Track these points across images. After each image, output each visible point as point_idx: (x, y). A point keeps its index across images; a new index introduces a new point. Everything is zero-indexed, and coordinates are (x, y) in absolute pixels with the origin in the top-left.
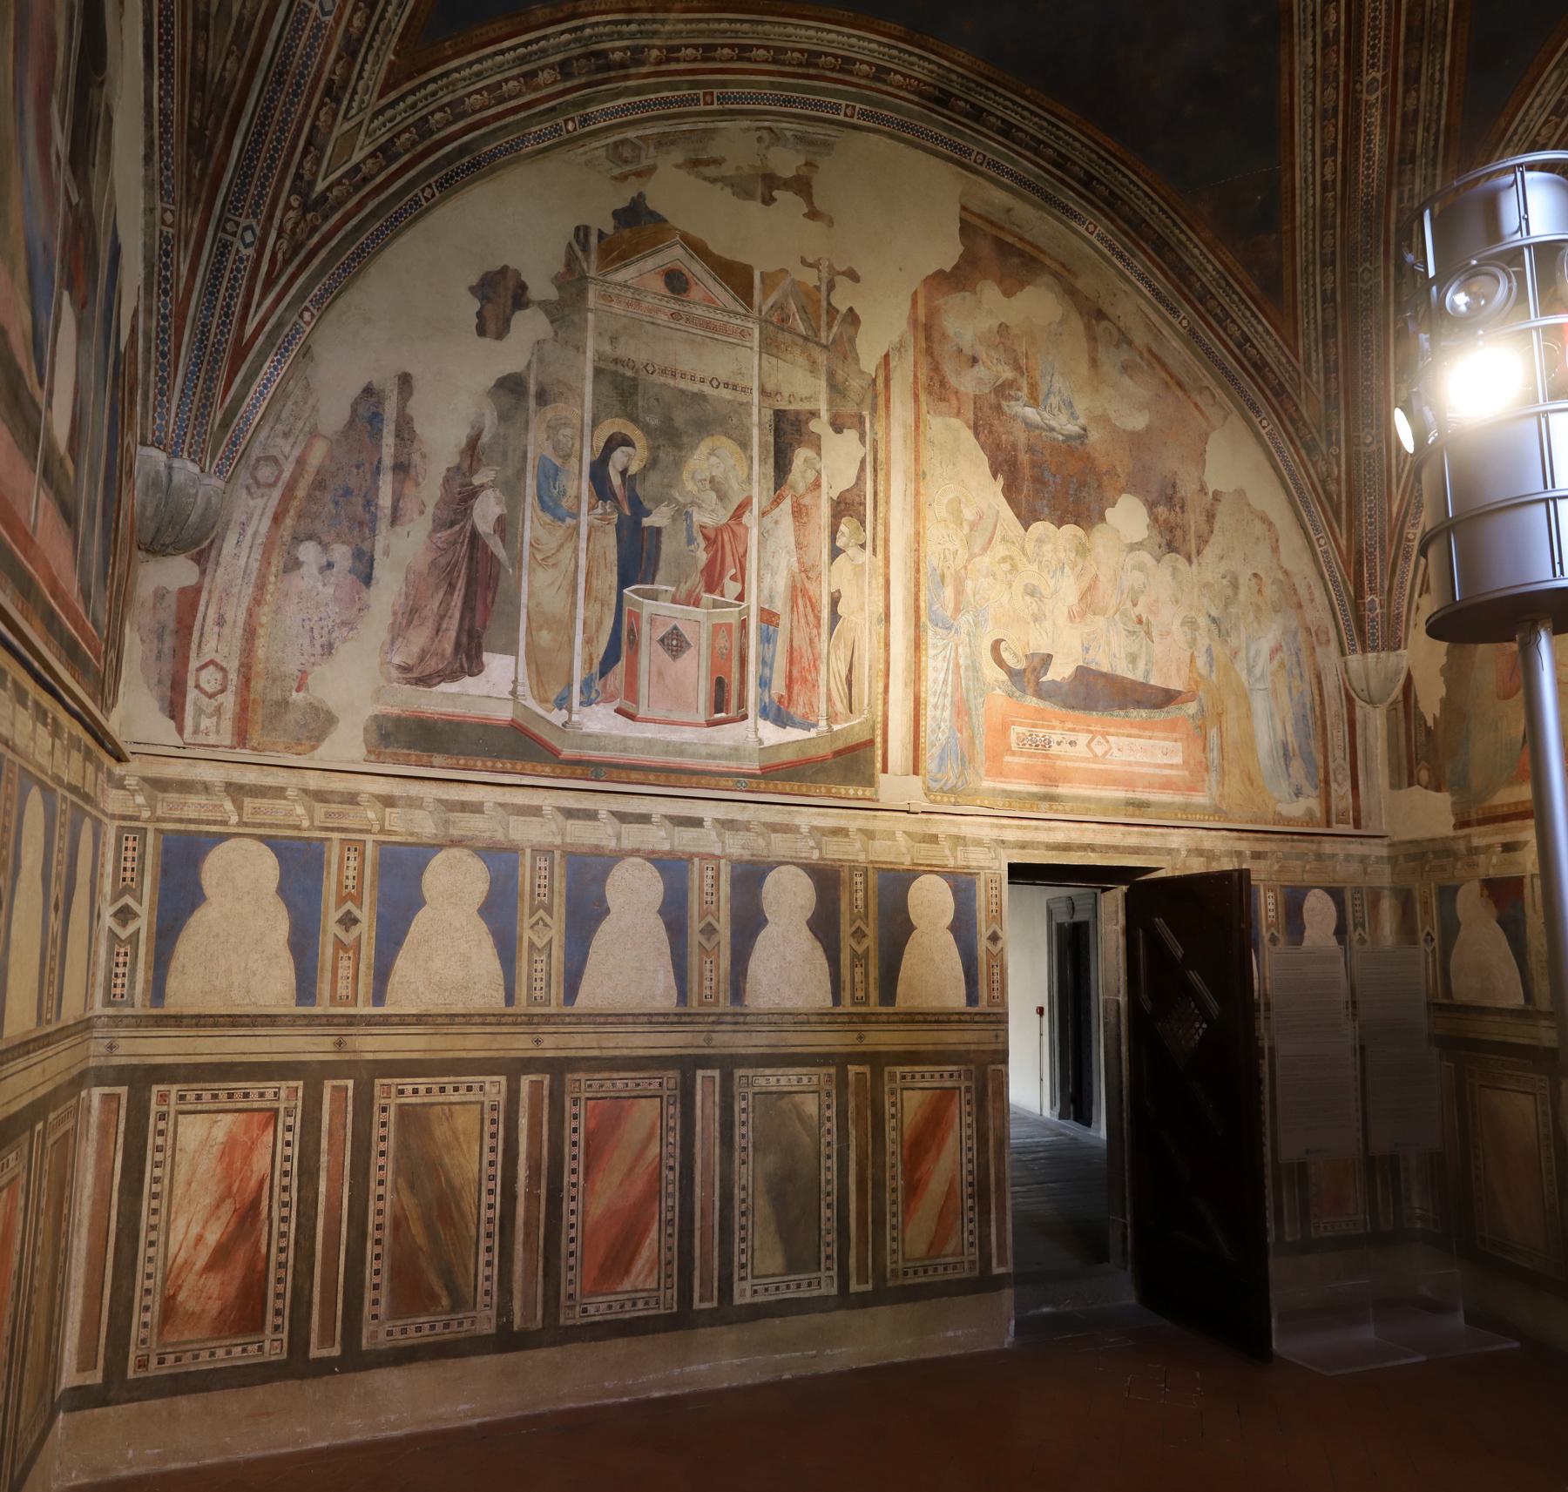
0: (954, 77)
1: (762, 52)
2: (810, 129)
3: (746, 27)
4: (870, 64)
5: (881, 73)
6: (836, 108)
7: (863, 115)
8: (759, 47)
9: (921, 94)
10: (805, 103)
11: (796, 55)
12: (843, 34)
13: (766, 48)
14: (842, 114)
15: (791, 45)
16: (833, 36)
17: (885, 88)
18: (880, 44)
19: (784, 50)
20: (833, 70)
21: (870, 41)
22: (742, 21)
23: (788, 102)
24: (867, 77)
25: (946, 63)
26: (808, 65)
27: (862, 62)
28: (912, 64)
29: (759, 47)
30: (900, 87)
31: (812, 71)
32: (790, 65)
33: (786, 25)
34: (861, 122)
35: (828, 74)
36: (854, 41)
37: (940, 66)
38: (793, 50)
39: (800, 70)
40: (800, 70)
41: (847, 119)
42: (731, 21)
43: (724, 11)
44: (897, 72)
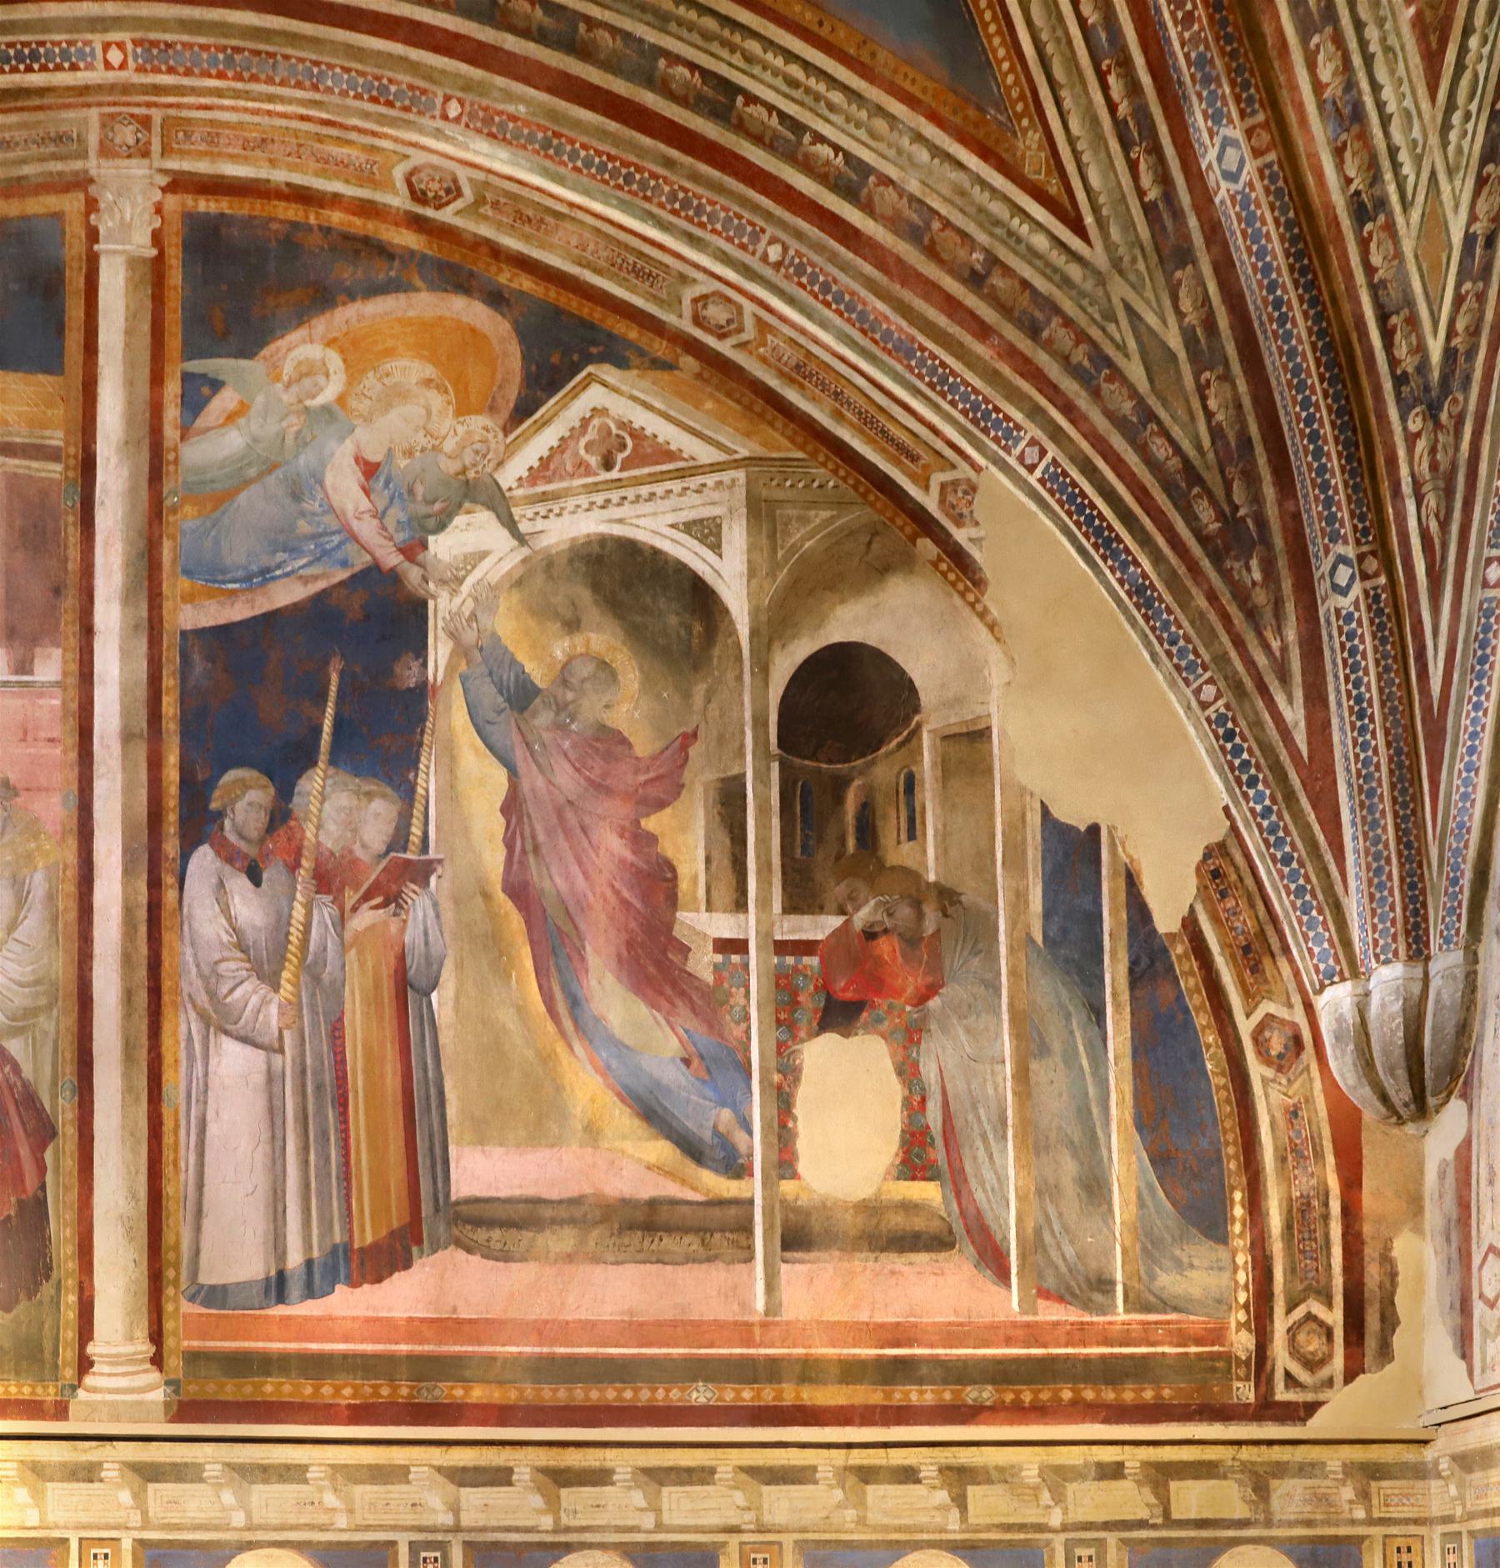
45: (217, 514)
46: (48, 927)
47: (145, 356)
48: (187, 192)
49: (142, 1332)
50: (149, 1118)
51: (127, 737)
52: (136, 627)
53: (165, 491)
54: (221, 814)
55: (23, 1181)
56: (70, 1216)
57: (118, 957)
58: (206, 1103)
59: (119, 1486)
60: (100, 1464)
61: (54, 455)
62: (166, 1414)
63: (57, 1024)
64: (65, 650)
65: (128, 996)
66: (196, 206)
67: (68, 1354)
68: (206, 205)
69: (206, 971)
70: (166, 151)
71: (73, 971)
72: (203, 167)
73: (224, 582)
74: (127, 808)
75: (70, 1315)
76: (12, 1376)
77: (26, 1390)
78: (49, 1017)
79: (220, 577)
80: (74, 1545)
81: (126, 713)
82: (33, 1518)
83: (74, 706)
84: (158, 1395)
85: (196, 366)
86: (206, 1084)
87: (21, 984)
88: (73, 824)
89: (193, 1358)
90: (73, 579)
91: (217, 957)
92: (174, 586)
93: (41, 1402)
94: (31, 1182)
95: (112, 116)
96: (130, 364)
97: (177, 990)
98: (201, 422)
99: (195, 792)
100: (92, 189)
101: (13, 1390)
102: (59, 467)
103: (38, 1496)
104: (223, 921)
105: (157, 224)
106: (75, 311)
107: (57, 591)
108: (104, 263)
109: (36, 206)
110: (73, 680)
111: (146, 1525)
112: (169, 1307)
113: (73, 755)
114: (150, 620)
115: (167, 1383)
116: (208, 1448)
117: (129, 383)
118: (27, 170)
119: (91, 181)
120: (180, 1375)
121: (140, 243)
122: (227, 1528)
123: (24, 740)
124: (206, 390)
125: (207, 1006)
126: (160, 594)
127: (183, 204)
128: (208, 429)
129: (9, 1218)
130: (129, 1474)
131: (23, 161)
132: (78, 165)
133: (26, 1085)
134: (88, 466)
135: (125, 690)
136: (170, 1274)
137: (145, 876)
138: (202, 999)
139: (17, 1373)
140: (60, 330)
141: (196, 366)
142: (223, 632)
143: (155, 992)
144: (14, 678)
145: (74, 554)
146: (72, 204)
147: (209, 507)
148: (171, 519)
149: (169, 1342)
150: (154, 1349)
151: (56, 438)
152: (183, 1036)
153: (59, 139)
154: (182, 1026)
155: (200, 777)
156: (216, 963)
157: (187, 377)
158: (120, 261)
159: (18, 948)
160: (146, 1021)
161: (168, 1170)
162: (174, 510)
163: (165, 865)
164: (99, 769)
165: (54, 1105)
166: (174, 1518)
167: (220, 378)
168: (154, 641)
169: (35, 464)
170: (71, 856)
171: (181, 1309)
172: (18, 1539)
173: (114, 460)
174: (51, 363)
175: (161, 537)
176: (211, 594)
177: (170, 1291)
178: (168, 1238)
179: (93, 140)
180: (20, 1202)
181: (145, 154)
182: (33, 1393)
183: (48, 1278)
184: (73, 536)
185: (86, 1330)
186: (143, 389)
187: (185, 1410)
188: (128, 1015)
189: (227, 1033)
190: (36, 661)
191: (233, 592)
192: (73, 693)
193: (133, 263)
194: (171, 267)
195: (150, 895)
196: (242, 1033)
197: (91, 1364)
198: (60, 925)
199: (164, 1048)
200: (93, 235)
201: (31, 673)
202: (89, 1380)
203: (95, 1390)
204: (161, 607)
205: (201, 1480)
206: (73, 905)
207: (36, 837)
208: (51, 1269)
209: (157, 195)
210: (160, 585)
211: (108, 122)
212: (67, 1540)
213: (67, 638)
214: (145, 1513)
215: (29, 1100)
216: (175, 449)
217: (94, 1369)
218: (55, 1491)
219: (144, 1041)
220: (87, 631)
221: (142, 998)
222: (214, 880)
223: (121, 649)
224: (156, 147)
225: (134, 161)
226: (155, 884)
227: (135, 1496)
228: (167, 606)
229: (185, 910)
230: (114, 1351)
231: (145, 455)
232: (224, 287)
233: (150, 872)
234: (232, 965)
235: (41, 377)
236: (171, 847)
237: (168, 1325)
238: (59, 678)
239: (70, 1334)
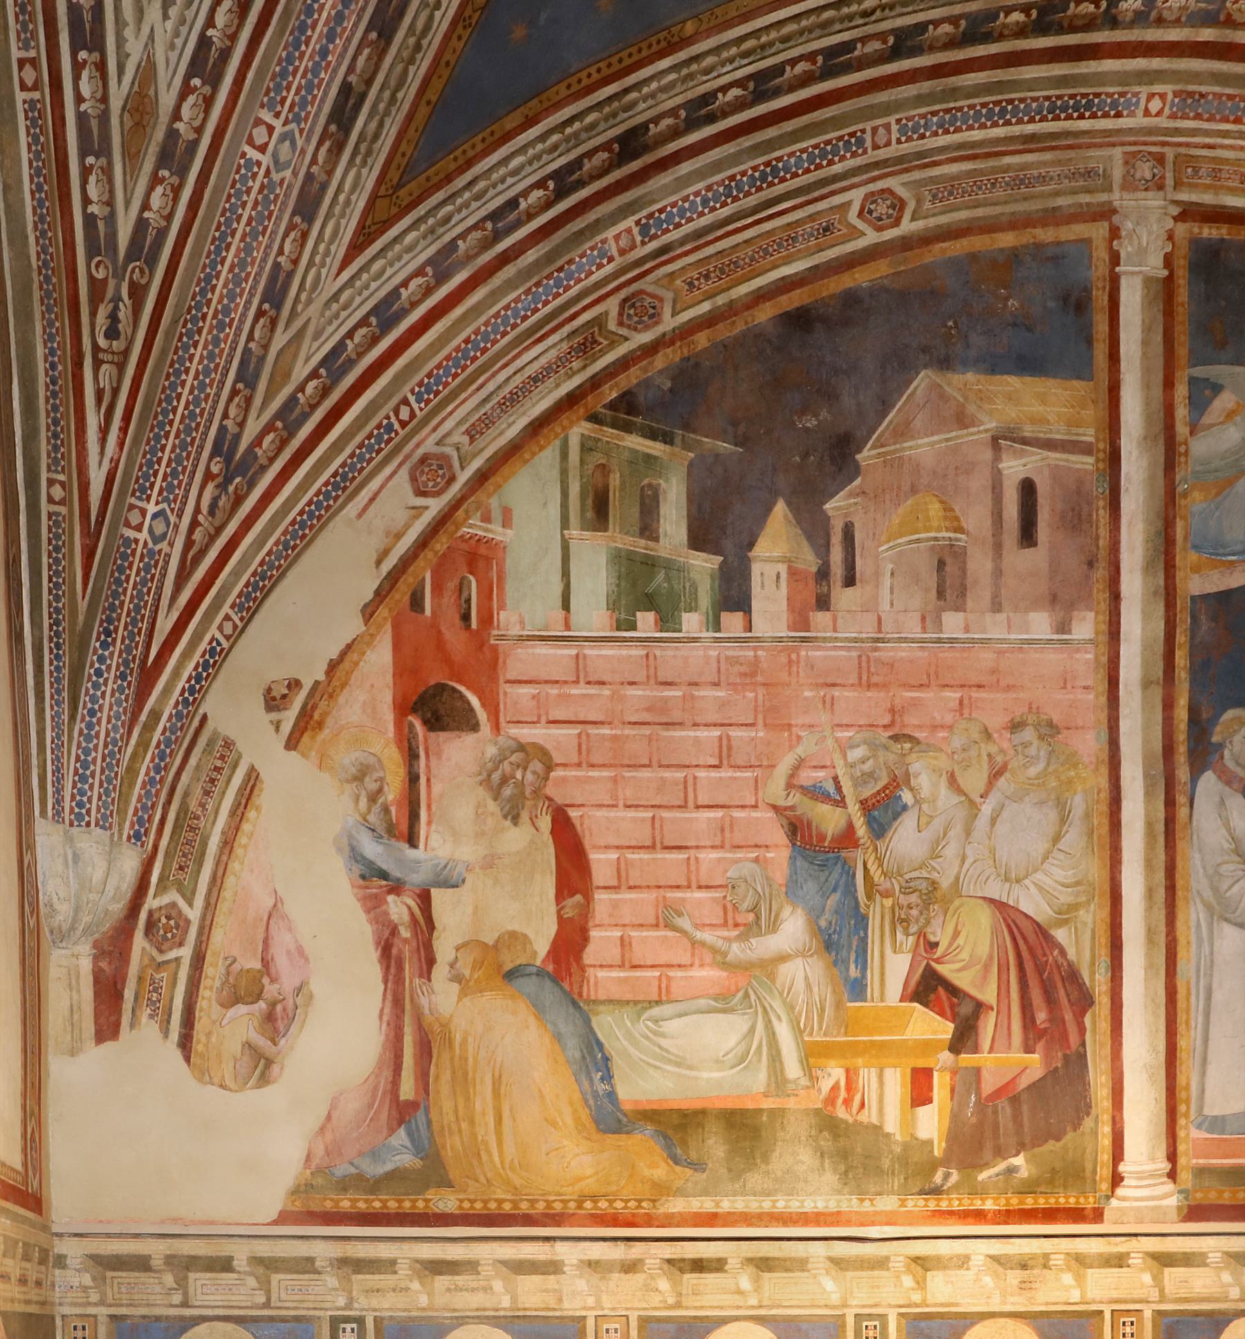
45: (1220, 498)
46: (1086, 839)
47: (1159, 363)
48: (1195, 221)
49: (1162, 1152)
50: (1166, 988)
51: (1146, 684)
52: (1155, 593)
53: (1178, 478)
54: (1220, 746)
55: (1067, 1040)
56: (1105, 1065)
57: (1142, 863)
58: (1211, 975)
59: (1142, 1270)
60: (1128, 1254)
61: (1087, 449)
62: (1179, 1215)
63: (1094, 917)
64: (1097, 613)
65: (1150, 893)
66: (1200, 233)
67: (1104, 1172)
68: (1209, 232)
69: (1211, 872)
70: (1178, 185)
71: (1106, 874)
72: (1207, 198)
73: (1225, 555)
74: (1146, 741)
75: (1106, 1142)
76: (1061, 1190)
77: (1072, 1200)
78: (1087, 911)
79: (1221, 551)
80: (1108, 1316)
81: (1146, 665)
82: (1075, 1296)
83: (1104, 659)
84: (1173, 1201)
85: (1199, 372)
86: (1212, 961)
87: (1063, 885)
88: (1105, 756)
89: (1200, 1172)
90: (1103, 553)
91: (1219, 860)
92: (1185, 558)
93: (1083, 1209)
94: (1073, 1039)
95: (1134, 154)
96: (1147, 371)
97: (1187, 889)
98: (1206, 420)
99: (1200, 728)
100: (1116, 219)
101: (1062, 1200)
102: (1091, 460)
103: (1080, 1279)
104: (1224, 831)
105: (1169, 249)
106: (1101, 327)
107: (1090, 564)
108: (1124, 282)
109: (1069, 232)
110: (1104, 638)
111: (1163, 1298)
112: (1181, 1134)
113: (1103, 700)
114: (1166, 587)
115: (1180, 1192)
116: (1211, 1241)
117: (1147, 386)
118: (1061, 201)
119: (1115, 211)
120: (1189, 1186)
121: (1154, 265)
122: (1226, 1299)
123: (1064, 688)
124: (1207, 392)
125: (1211, 899)
126: (1174, 566)
127: (1191, 232)
128: (1211, 426)
129: (1056, 1069)
130: (1150, 1261)
131: (1057, 194)
132: (1104, 197)
133: (1070, 965)
134: (1114, 458)
135: (1146, 647)
136: (1182, 1108)
137: (1162, 797)
138: (1208, 894)
139: (1065, 1187)
140: (1089, 341)
141: (1199, 372)
142: (1224, 598)
143: (1171, 889)
144: (1055, 637)
145: (1104, 532)
146: (1098, 232)
147: (1214, 491)
148: (1183, 502)
149: (1182, 1161)
150: (1169, 1166)
151: (1088, 435)
152: (1193, 924)
153: (1088, 173)
154: (1192, 915)
155: (1204, 716)
156: (1219, 865)
157: (1193, 381)
158: (1137, 282)
159: (1061, 856)
160: (1164, 912)
161: (1181, 1028)
162: (1185, 495)
163: (1179, 788)
164: (1124, 710)
165: (1092, 980)
166: (1183, 1293)
167: (1220, 382)
168: (1170, 605)
169: (1072, 458)
170: (1104, 781)
171: (1190, 1134)
172: (1064, 1312)
173: (1135, 453)
174: (1081, 371)
175: (1175, 517)
176: (1214, 565)
177: (1182, 1121)
178: (1181, 1080)
179: (1117, 173)
180: (1066, 1057)
181: (1161, 187)
182: (1077, 1202)
183: (1088, 1114)
184: (1103, 516)
185: (1118, 1154)
186: (1158, 392)
187: (1194, 1212)
188: (1149, 908)
189: (1226, 920)
190: (1074, 622)
191: (1232, 562)
192: (1104, 649)
193: (1148, 281)
194: (1179, 286)
195: (1166, 811)
196: (1239, 920)
197: (1122, 1179)
198: (1095, 838)
199: (1178, 933)
200: (1115, 259)
201: (1069, 632)
202: (1120, 1191)
203: (1124, 1199)
204: (1174, 577)
205: (1206, 1265)
206: (1106, 821)
207: (1075, 766)
208: (1090, 1107)
209: (1170, 224)
210: (1174, 557)
211: (1130, 160)
212: (1102, 1312)
213: (1099, 603)
214: (1162, 1291)
215: (1073, 976)
216: (1186, 443)
217: (1124, 1183)
218: (1093, 1274)
219: (1162, 928)
220: (1116, 597)
221: (1161, 894)
222: (1217, 799)
223: (1143, 612)
224: (1169, 181)
225: (1150, 194)
226: (1170, 803)
227: (1154, 1278)
228: (1179, 575)
229: (1194, 823)
230: (1139, 1168)
231: (1161, 448)
232: (1223, 303)
233: (1167, 793)
234: (1231, 867)
235: (1075, 383)
236: (1183, 773)
237: (1181, 1148)
238: (1092, 636)
239: (1106, 1157)
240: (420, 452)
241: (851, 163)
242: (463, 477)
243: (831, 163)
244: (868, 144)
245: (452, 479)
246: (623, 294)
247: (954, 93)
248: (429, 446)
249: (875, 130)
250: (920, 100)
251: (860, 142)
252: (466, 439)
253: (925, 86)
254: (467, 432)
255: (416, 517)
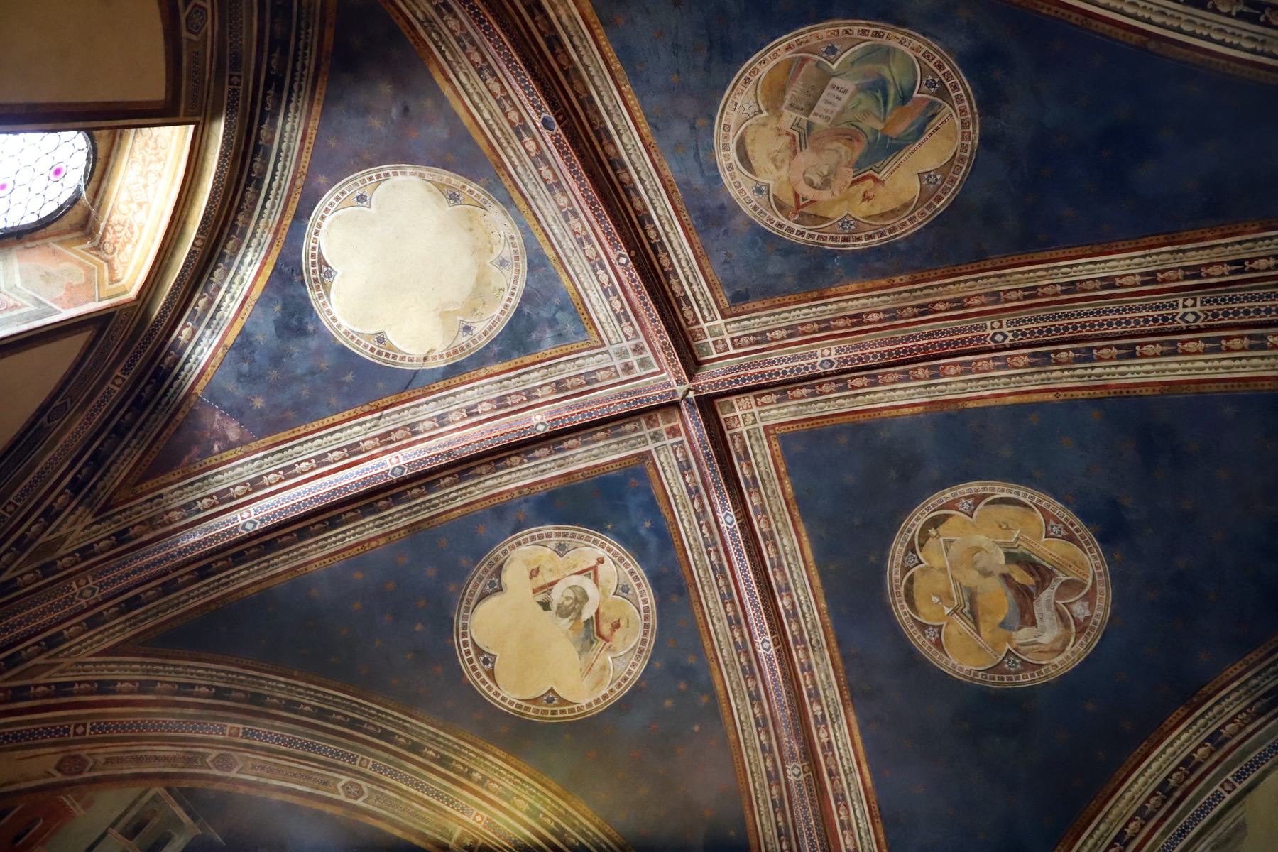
0: (1254, 682)
1: (1132, 826)
2: (1220, 830)
3: (1102, 827)
4: (1202, 745)
5: (1215, 740)
6: (1218, 797)
7: (1239, 777)
8: (1126, 826)
9: (1260, 714)
10: (1195, 820)
11: (1153, 801)
12: (1159, 756)
13: (1131, 820)
14: (1226, 795)
15: (1142, 800)
16: (1155, 766)
17: (1234, 741)
18: (1185, 730)
19: (1143, 807)
20: (1187, 777)
21: (1178, 737)
22: (1097, 828)
23: (1183, 833)
24: (1212, 753)
25: (1236, 684)
26: (1169, 795)
27: (1195, 751)
28: (1221, 712)
29: (1126, 826)
30: (1241, 729)
31: (1177, 794)
32: (1158, 809)
33: (1121, 797)
34: (1245, 783)
35: (1188, 782)
36: (1169, 751)
37: (1236, 689)
38: (1147, 800)
39: (1169, 804)
40: (1169, 804)
41: (1234, 793)
42: (1090, 836)
43: (1079, 836)
44: (1223, 726)
240: (78, 753)
241: (347, 764)
242: (86, 775)
243: (339, 759)
244: (358, 762)
245: (80, 772)
246: (223, 752)
247: (401, 766)
248: (83, 753)
249: (362, 759)
250: (387, 761)
251: (355, 760)
252: (103, 761)
253: (391, 757)
254: (107, 759)
255: (45, 777)
